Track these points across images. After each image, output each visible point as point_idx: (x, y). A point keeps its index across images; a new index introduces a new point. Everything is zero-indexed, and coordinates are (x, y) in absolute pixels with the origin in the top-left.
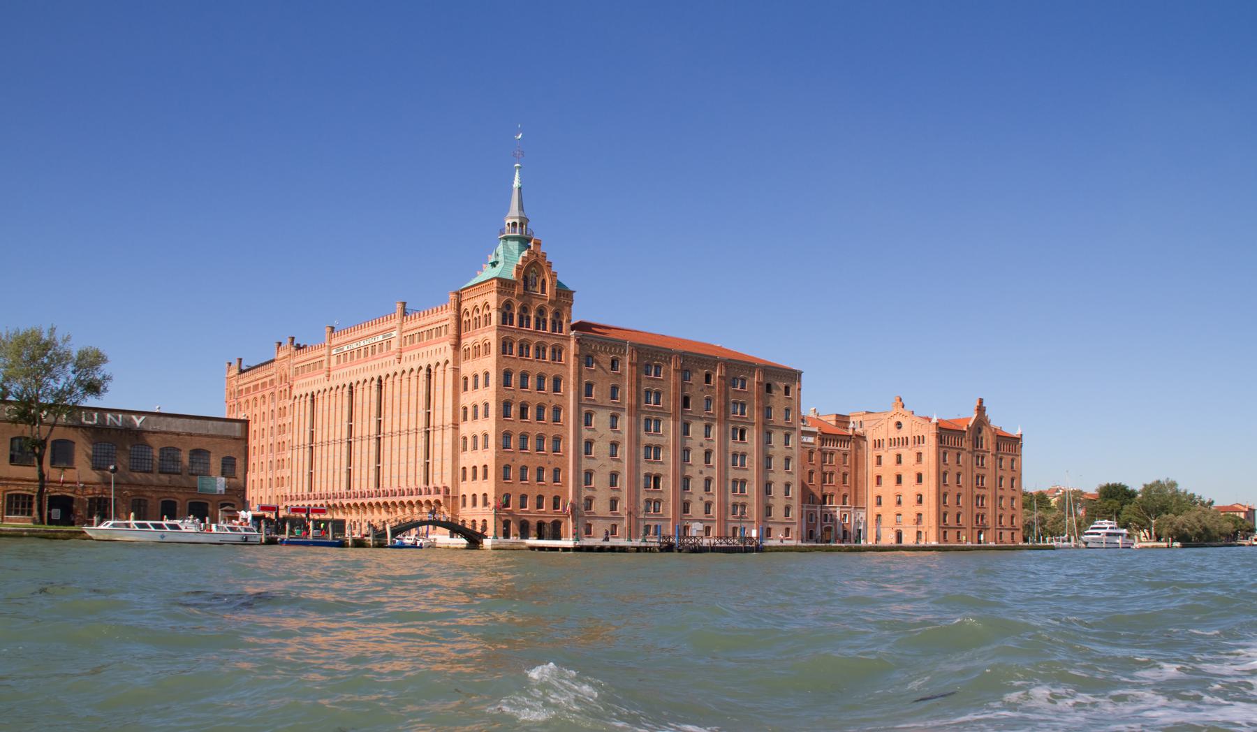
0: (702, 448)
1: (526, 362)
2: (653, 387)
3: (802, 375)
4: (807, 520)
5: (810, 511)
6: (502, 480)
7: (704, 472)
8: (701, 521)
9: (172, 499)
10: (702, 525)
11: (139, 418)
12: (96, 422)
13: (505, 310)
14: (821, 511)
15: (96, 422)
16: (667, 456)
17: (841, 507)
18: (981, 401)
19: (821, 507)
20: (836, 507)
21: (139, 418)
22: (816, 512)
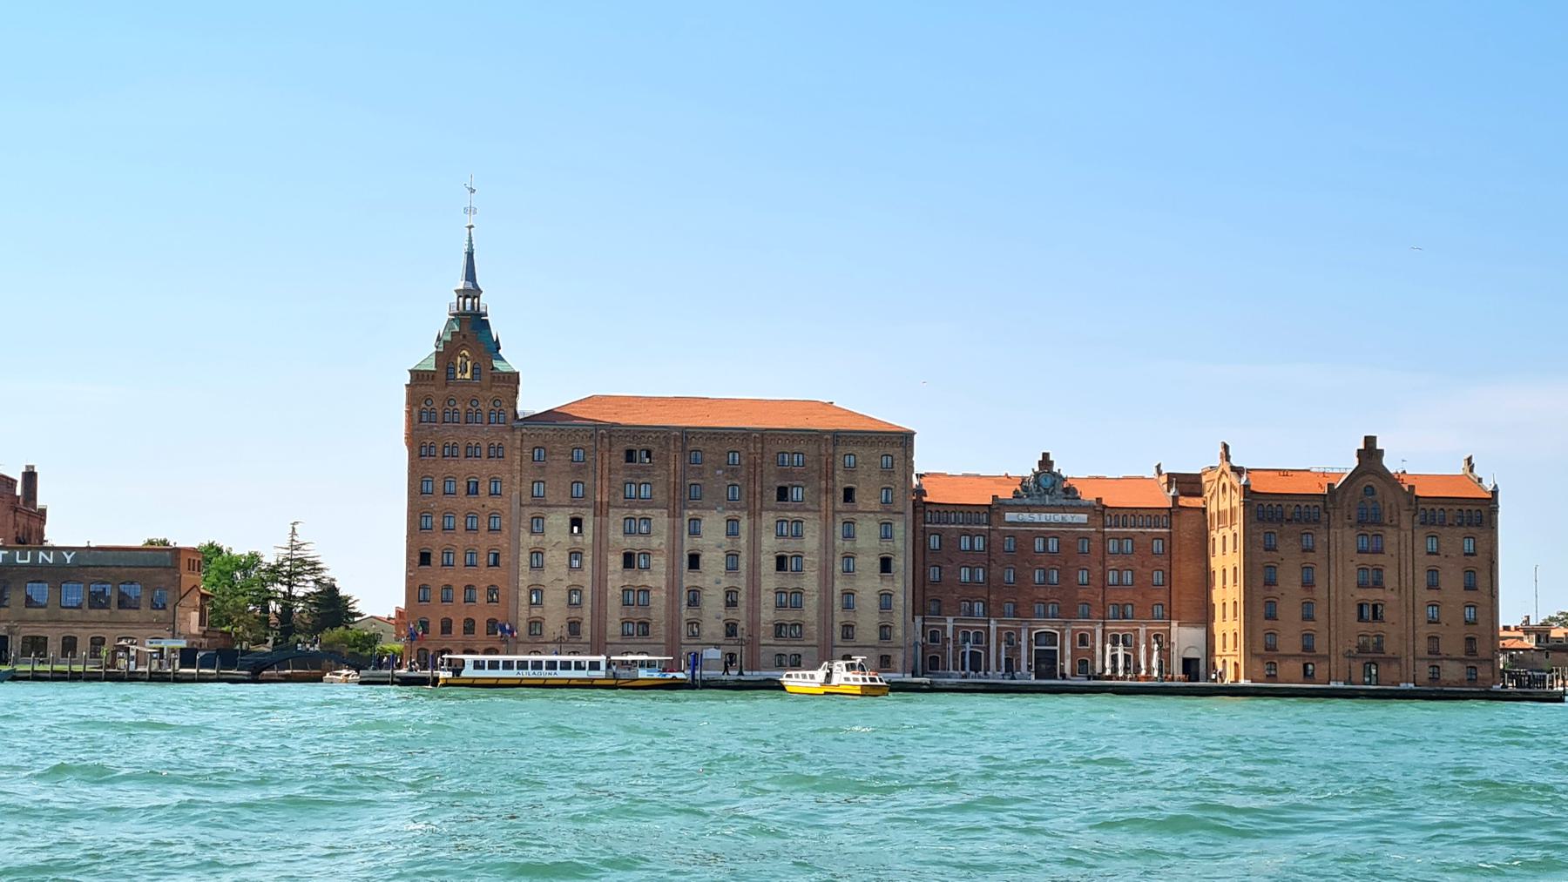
0: (720, 550)
1: (452, 463)
2: (638, 477)
3: (915, 436)
4: (1073, 644)
5: (1081, 630)
6: (416, 603)
7: (722, 582)
8: (717, 646)
9: (103, 636)
10: (720, 651)
11: (69, 554)
12: (28, 561)
13: (423, 405)
14: (1103, 631)
15: (28, 561)
16: (659, 563)
17: (1147, 624)
18: (1370, 441)
19: (1104, 624)
20: (1140, 624)
21: (69, 554)
22: (1093, 632)
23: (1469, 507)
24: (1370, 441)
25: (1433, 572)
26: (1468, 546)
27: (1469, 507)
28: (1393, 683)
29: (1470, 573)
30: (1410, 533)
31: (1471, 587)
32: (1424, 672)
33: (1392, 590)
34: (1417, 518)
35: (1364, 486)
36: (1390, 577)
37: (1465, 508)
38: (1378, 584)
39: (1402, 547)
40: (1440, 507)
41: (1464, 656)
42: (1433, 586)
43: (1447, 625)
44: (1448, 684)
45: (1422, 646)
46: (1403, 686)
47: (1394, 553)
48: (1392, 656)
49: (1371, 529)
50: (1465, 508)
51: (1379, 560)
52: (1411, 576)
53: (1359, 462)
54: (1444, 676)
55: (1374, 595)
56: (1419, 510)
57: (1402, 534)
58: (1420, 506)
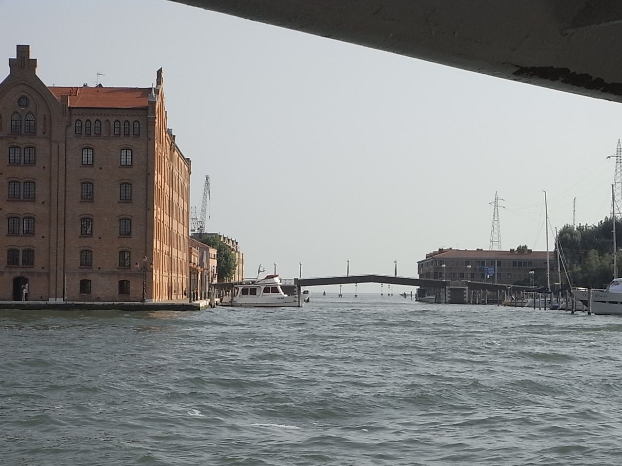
18: (23, 50)
23: (126, 118)
24: (23, 50)
25: (87, 184)
26: (126, 157)
27: (126, 118)
28: (41, 299)
29: (126, 185)
30: (62, 146)
31: (126, 200)
32: (73, 286)
33: (43, 203)
34: (71, 130)
35: (18, 97)
36: (41, 190)
37: (122, 120)
38: (31, 198)
39: (54, 159)
40: (95, 118)
41: (116, 270)
42: (88, 197)
43: (100, 238)
44: (99, 298)
45: (74, 259)
46: (52, 301)
47: (46, 165)
48: (43, 271)
49: (22, 141)
50: (122, 120)
51: (30, 172)
52: (62, 188)
53: (35, 75)
54: (96, 291)
55: (29, 208)
56: (73, 123)
57: (55, 146)
58: (75, 118)
